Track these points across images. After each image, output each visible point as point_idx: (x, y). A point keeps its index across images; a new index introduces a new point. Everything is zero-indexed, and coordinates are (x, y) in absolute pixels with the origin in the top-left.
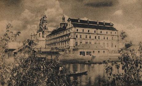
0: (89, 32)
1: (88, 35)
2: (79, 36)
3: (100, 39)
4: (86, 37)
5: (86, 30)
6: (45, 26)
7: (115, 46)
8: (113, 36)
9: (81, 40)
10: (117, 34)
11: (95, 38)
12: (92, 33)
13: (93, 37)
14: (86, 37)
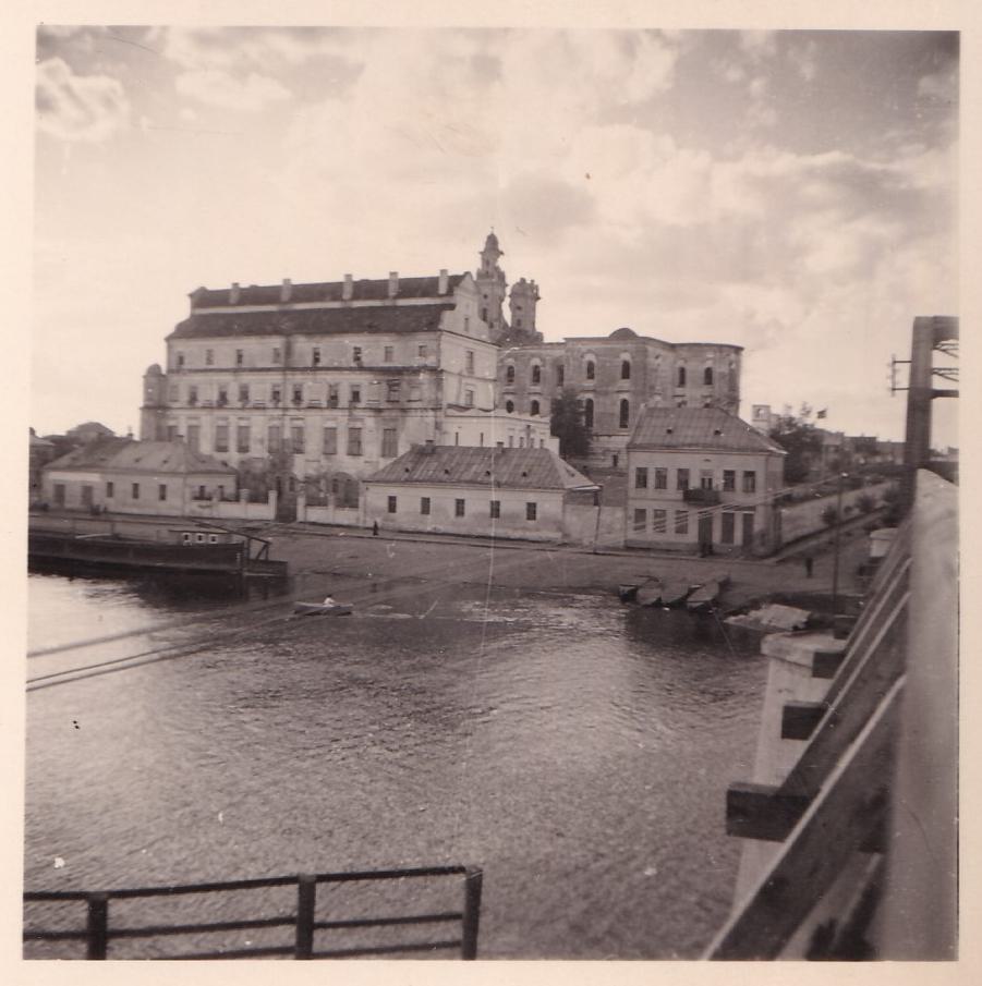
0: (240, 358)
3: (305, 404)
5: (225, 350)
10: (430, 361)
11: (276, 395)
12: (260, 365)
13: (261, 387)
14: (223, 397)
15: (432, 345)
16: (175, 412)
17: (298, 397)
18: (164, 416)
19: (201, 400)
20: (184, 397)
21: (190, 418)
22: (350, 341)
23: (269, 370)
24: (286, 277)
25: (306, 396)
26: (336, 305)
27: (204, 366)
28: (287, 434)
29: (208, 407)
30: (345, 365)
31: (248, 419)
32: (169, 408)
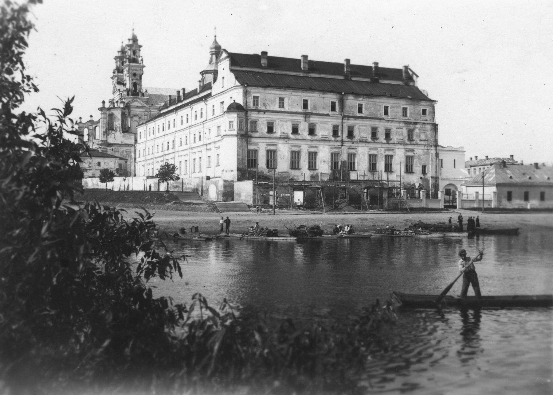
0: (305, 106)
1: (301, 118)
2: (263, 128)
3: (357, 138)
4: (295, 131)
6: (135, 85)
7: (424, 167)
8: (412, 127)
9: (275, 141)
11: (335, 133)
14: (295, 131)
15: (428, 109)
16: (254, 140)
17: (351, 134)
18: (248, 143)
19: (278, 132)
20: (263, 128)
21: (268, 144)
22: (383, 102)
23: (328, 115)
24: (265, 50)
25: (356, 133)
26: (342, 78)
27: (277, 108)
29: (285, 138)
30: (379, 116)
31: (316, 147)
32: (251, 137)
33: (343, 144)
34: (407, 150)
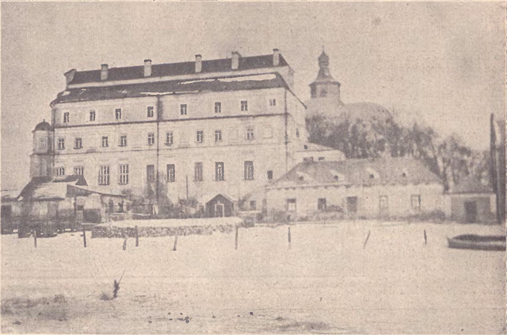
2: (70, 143)
16: (62, 158)
17: (169, 141)
19: (86, 145)
20: (70, 143)
28: (163, 169)
29: (92, 151)
33: (159, 153)
34: (245, 153)
